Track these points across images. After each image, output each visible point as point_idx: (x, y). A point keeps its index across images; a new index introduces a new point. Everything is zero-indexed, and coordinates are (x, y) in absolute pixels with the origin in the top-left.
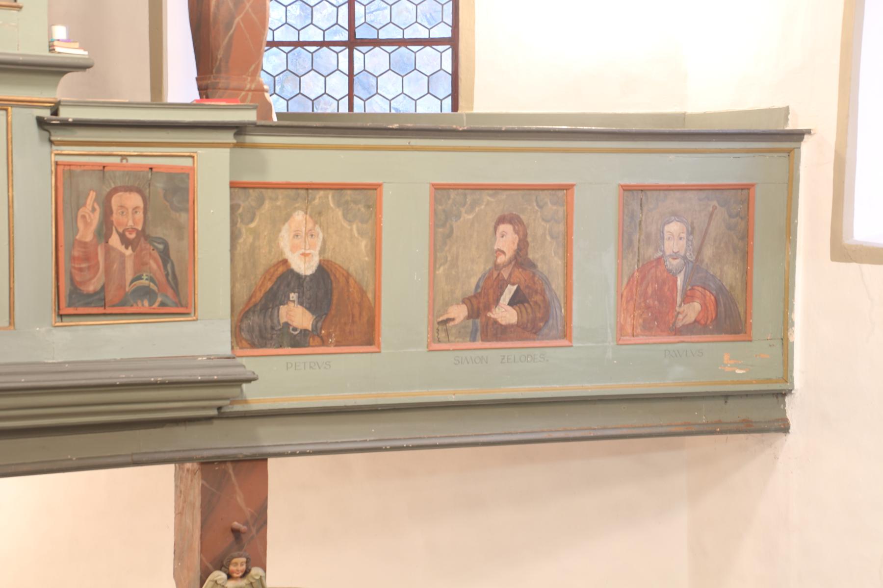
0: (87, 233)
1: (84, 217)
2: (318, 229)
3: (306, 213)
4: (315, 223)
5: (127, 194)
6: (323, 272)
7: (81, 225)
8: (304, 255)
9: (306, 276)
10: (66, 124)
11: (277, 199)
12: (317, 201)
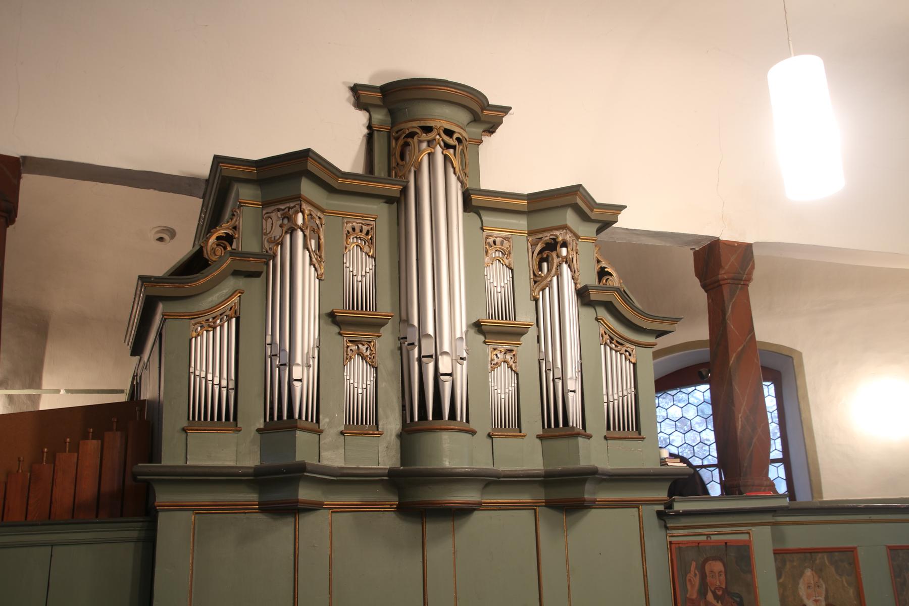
0: (693, 594)
1: (690, 580)
4: (819, 577)
5: (714, 563)
7: (689, 587)
8: (816, 601)
10: (678, 515)
12: (818, 561)
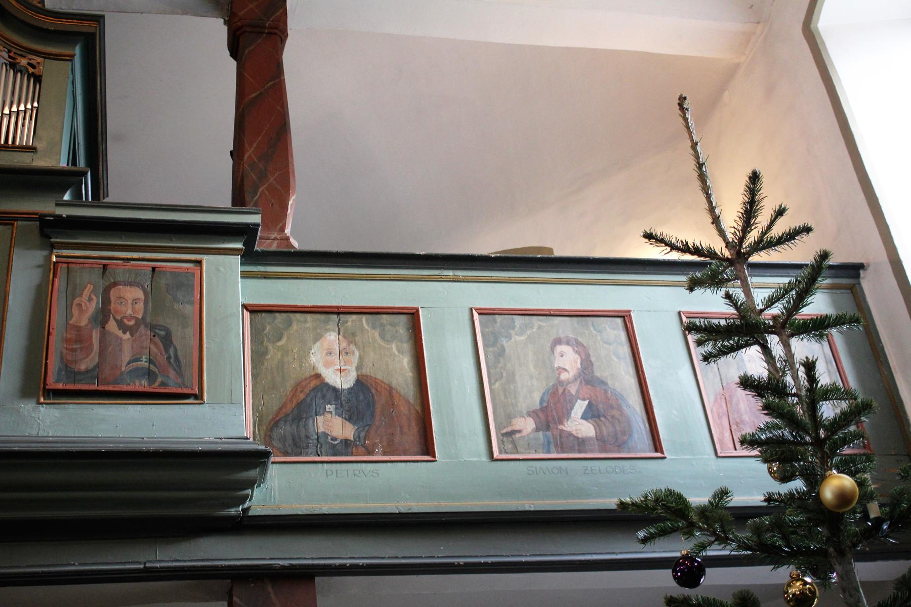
1: (80, 305)
2: (352, 347)
3: (339, 334)
4: (350, 343)
5: (128, 288)
6: (362, 384)
7: (75, 311)
9: (343, 390)
11: (305, 321)
12: (349, 324)
